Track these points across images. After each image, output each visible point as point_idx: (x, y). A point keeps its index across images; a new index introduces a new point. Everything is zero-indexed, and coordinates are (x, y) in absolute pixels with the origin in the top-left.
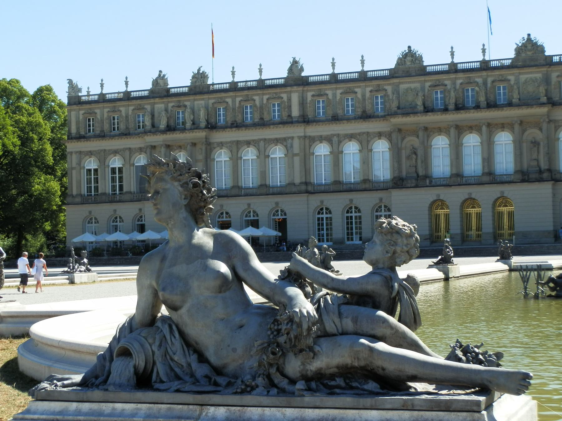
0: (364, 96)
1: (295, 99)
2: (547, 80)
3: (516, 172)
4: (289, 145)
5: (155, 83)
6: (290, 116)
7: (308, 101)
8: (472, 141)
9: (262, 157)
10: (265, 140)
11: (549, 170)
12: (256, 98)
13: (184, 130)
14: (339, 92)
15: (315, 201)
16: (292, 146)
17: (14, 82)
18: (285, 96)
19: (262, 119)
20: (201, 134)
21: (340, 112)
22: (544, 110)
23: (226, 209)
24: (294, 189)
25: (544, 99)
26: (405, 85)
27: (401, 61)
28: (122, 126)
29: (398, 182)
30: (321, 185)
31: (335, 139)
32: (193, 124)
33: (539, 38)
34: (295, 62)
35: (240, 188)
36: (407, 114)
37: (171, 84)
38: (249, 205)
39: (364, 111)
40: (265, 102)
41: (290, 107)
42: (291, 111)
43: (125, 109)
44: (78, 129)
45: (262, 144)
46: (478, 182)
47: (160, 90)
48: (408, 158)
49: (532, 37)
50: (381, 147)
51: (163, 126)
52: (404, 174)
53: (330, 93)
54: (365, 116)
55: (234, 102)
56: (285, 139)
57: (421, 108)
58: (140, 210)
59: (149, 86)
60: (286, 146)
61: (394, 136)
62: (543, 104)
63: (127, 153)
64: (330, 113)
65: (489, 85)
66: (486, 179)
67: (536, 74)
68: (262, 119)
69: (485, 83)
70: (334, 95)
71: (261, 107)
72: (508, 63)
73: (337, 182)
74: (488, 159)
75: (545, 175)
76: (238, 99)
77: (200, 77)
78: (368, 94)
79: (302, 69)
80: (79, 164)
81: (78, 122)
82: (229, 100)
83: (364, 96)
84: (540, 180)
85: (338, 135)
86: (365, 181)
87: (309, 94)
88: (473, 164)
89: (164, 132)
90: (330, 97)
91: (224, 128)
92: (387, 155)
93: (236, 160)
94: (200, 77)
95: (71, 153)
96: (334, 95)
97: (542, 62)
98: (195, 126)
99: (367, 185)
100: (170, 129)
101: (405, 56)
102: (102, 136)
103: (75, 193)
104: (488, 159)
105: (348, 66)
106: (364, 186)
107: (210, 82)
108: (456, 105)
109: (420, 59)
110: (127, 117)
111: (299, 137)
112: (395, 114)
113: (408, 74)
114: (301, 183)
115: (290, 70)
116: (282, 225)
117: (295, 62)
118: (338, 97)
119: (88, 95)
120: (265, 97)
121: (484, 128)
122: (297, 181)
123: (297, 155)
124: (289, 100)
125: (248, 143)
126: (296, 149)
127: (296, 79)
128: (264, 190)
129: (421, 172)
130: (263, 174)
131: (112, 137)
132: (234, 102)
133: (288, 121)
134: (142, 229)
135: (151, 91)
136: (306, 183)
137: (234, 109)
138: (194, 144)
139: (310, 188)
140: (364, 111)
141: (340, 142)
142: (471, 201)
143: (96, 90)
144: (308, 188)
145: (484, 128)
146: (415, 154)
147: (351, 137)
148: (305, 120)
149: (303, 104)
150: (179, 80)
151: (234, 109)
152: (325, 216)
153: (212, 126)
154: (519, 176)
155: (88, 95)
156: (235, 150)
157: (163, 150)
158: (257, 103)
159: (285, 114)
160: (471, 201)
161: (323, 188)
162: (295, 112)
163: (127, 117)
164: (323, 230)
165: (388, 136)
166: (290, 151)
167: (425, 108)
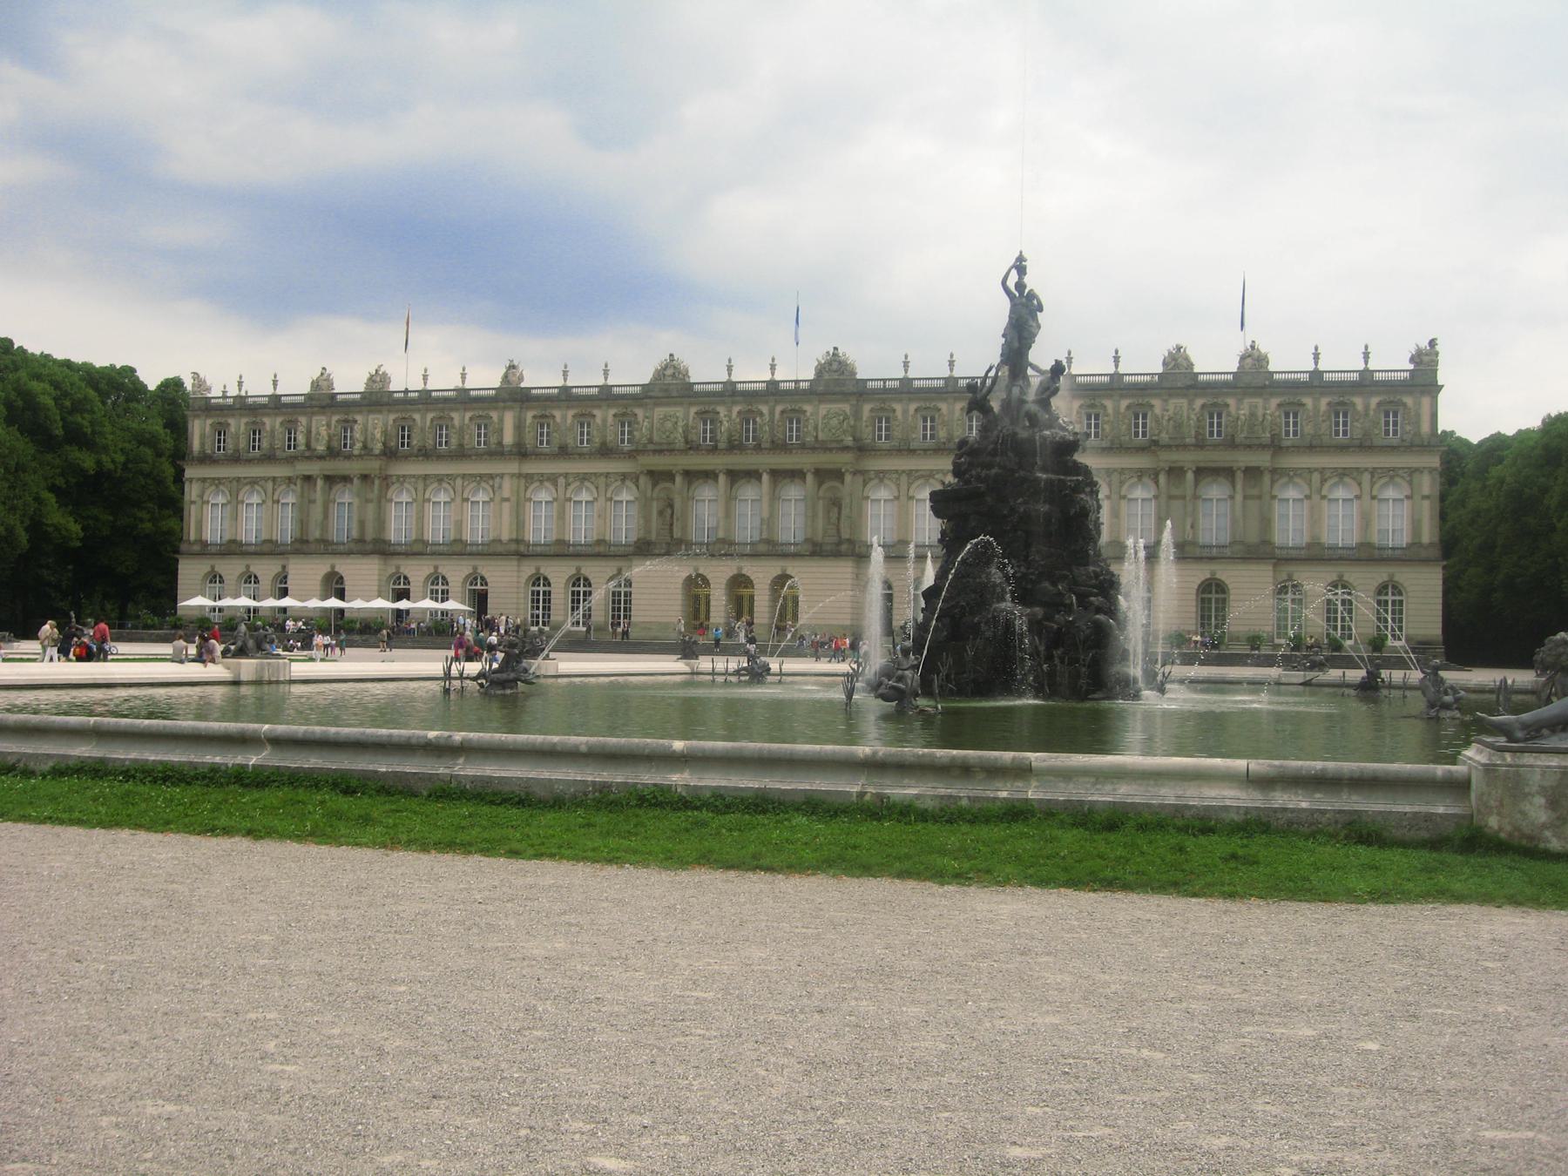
0: (604, 421)
1: (509, 420)
2: (857, 414)
3: (807, 540)
5: (315, 385)
6: (500, 443)
8: (748, 492)
9: (459, 500)
10: (464, 476)
11: (849, 541)
12: (455, 415)
13: (349, 457)
14: (571, 413)
15: (528, 569)
16: (500, 487)
17: (129, 371)
18: (494, 415)
19: (461, 445)
20: (373, 466)
21: (570, 441)
22: (847, 457)
23: (405, 570)
24: (500, 549)
25: (849, 440)
27: (660, 374)
28: (265, 444)
29: (642, 549)
30: (400, 544)
31: (561, 481)
32: (365, 447)
33: (850, 353)
34: (512, 367)
35: (426, 543)
36: (660, 452)
37: (339, 387)
38: (436, 568)
39: (604, 444)
41: (501, 431)
43: (272, 423)
44: (202, 444)
45: (459, 482)
47: (322, 400)
48: (661, 513)
49: (840, 352)
51: (321, 448)
52: (653, 537)
53: (558, 414)
54: (605, 451)
55: (423, 418)
56: (492, 477)
57: (680, 442)
58: (284, 567)
59: (306, 389)
61: (642, 480)
62: (846, 449)
63: (270, 485)
64: (556, 441)
65: (777, 416)
66: (762, 548)
68: (461, 445)
69: (772, 413)
70: (564, 418)
71: (461, 429)
72: (803, 385)
73: (561, 542)
74: (769, 522)
75: (844, 547)
76: (430, 416)
77: (378, 379)
78: (610, 419)
79: (521, 379)
80: (201, 496)
81: (203, 436)
82: (417, 417)
83: (604, 421)
84: (836, 554)
85: (566, 475)
86: (600, 542)
87: (529, 415)
88: (747, 528)
89: (321, 458)
90: (558, 419)
91: (406, 457)
92: (634, 510)
94: (378, 379)
95: (191, 480)
96: (564, 418)
97: (851, 388)
99: (601, 551)
101: (665, 368)
102: (236, 459)
103: (192, 537)
104: (769, 522)
106: (597, 549)
107: (392, 388)
108: (730, 441)
109: (686, 374)
110: (272, 431)
111: (512, 475)
112: (643, 452)
114: (511, 540)
115: (506, 376)
116: (480, 601)
117: (512, 367)
119: (224, 397)
120: (468, 415)
121: (765, 477)
122: (505, 537)
123: (507, 500)
124: (501, 420)
125: (440, 479)
128: (458, 548)
129: (677, 534)
130: (459, 525)
131: (249, 461)
132: (423, 418)
133: (498, 453)
134: (284, 593)
135: (309, 397)
136: (518, 541)
137: (423, 429)
138: (365, 478)
139: (522, 548)
140: (604, 444)
141: (568, 485)
142: (739, 583)
143: (233, 391)
144: (519, 551)
145: (765, 477)
146: (671, 506)
147: (584, 478)
148: (521, 452)
149: (519, 427)
150: (350, 381)
151: (423, 429)
152: (541, 589)
153: (390, 454)
154: (807, 548)
155: (224, 397)
156: (420, 486)
157: (320, 483)
158: (456, 422)
159: (493, 440)
161: (539, 549)
162: (508, 438)
163: (272, 431)
167: (687, 442)
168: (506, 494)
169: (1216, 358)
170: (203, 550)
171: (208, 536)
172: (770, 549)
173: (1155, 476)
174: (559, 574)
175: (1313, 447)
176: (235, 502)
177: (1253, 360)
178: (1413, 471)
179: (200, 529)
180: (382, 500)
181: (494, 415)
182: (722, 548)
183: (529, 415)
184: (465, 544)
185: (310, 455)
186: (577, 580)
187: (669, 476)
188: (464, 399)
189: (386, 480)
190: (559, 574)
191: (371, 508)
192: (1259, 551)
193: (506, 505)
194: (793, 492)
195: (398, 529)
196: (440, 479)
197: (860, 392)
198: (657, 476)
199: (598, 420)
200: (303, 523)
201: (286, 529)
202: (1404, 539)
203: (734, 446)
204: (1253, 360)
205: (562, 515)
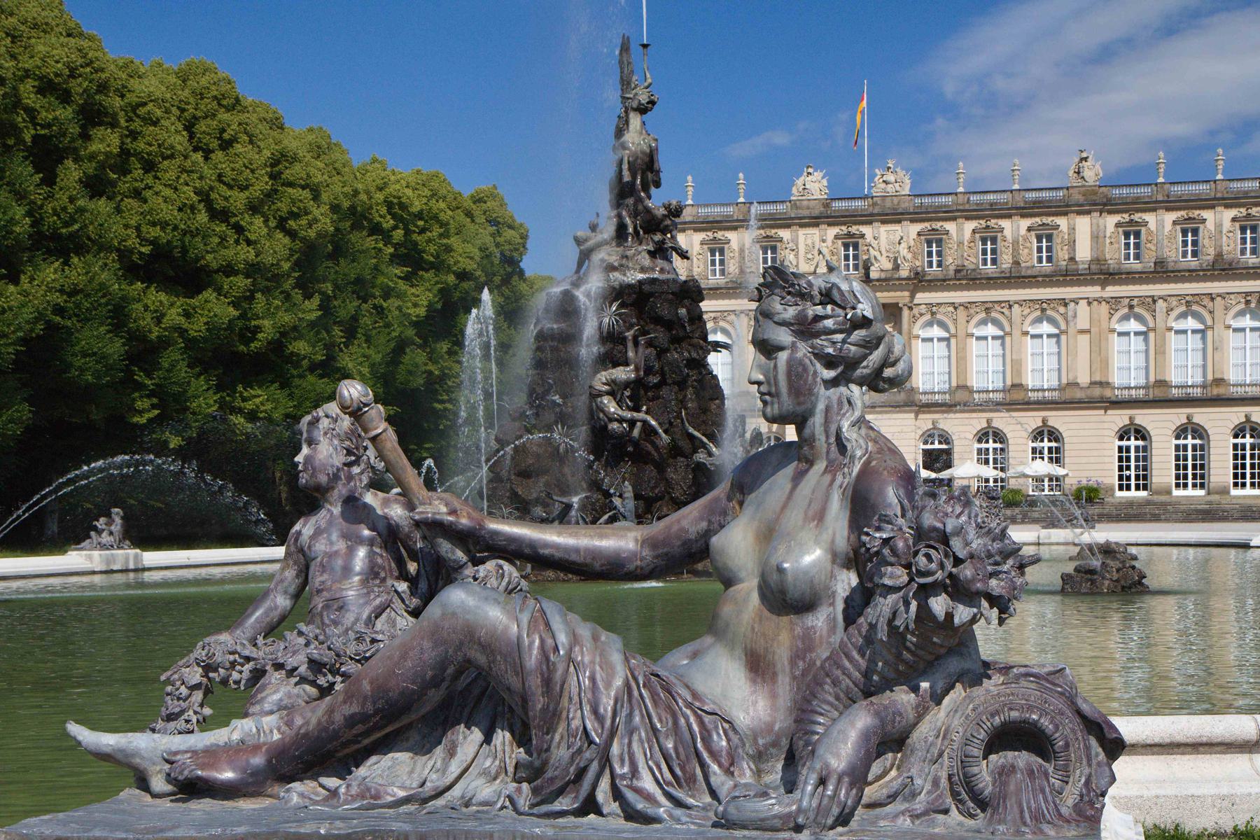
0: (1219, 226)
4: (1070, 313)
6: (1072, 259)
7: (1108, 235)
15: (1120, 418)
16: (1075, 316)
19: (1017, 263)
24: (1079, 395)
28: (732, 267)
31: (1161, 304)
39: (1219, 255)
40: (1023, 231)
42: (1074, 250)
60: (1065, 316)
68: (1017, 263)
70: (1160, 224)
71: (1015, 243)
78: (1227, 224)
83: (1219, 226)
90: (1152, 225)
110: (742, 251)
114: (1093, 383)
118: (1168, 227)
122: (1084, 379)
123: (1082, 332)
124: (1072, 229)
126: (1083, 321)
130: (1017, 366)
132: (960, 230)
137: (960, 243)
139: (1108, 393)
140: (1219, 255)
149: (1096, 237)
151: (960, 243)
162: (1084, 253)
164: (1128, 468)
166: (1071, 324)
168: (1083, 323)
174: (1161, 425)
181: (1062, 222)
183: (1111, 221)
184: (971, 391)
186: (1189, 429)
190: (1161, 425)
193: (1084, 340)
196: (988, 307)
199: (1210, 225)
205: (1161, 351)
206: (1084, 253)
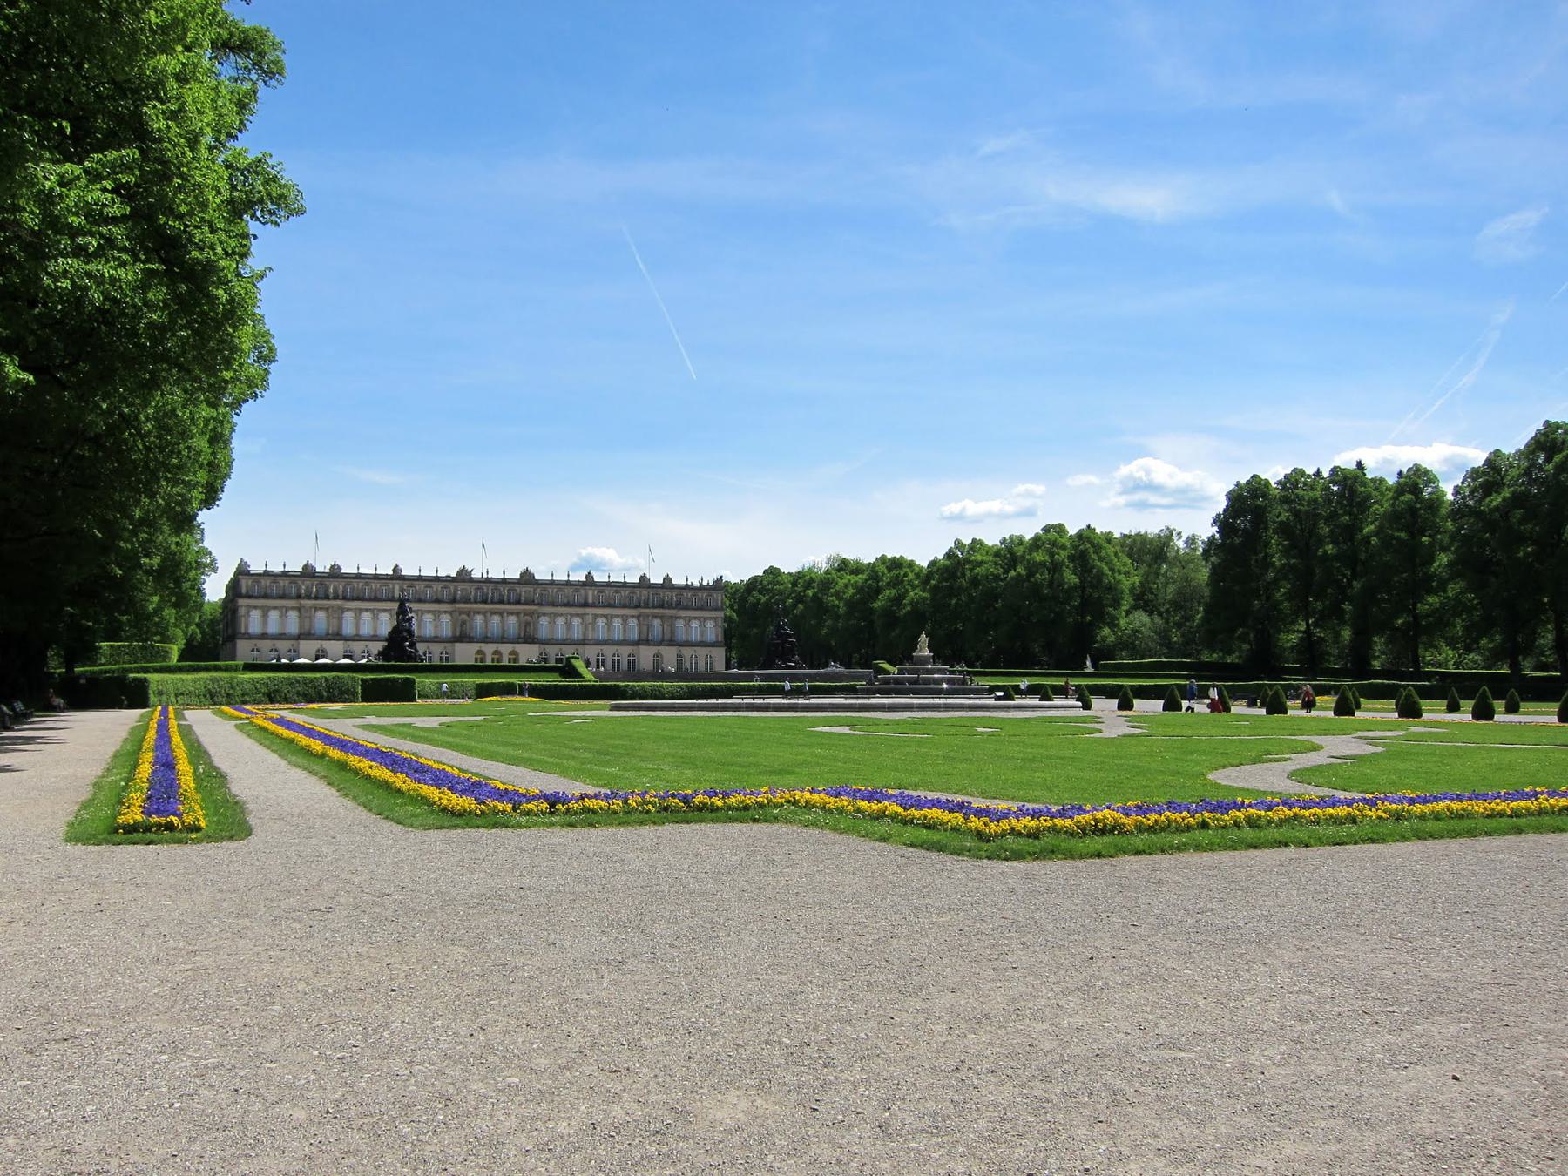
1: (397, 587)
5: (305, 567)
8: (496, 619)
13: (327, 598)
26: (461, 586)
43: (284, 582)
46: (299, 637)
47: (308, 572)
50: (446, 618)
54: (438, 601)
67: (530, 588)
93: (357, 619)
98: (336, 597)
100: (316, 598)
105: (428, 572)
113: (463, 581)
127: (397, 575)
142: (497, 652)
149: (402, 590)
150: (322, 567)
160: (497, 652)
162: (397, 595)
165: (451, 613)
169: (656, 579)
170: (250, 637)
171: (251, 631)
172: (503, 639)
173: (638, 617)
175: (686, 608)
176: (265, 615)
177: (667, 579)
178: (715, 619)
179: (247, 627)
180: (340, 619)
182: (486, 639)
185: (308, 597)
187: (468, 613)
188: (376, 577)
189: (343, 610)
191: (335, 622)
192: (672, 642)
194: (513, 619)
195: (348, 629)
197: (538, 583)
198: (461, 613)
200: (301, 626)
201: (293, 626)
202: (713, 638)
203: (492, 602)
204: (667, 579)
206: (397, 595)
